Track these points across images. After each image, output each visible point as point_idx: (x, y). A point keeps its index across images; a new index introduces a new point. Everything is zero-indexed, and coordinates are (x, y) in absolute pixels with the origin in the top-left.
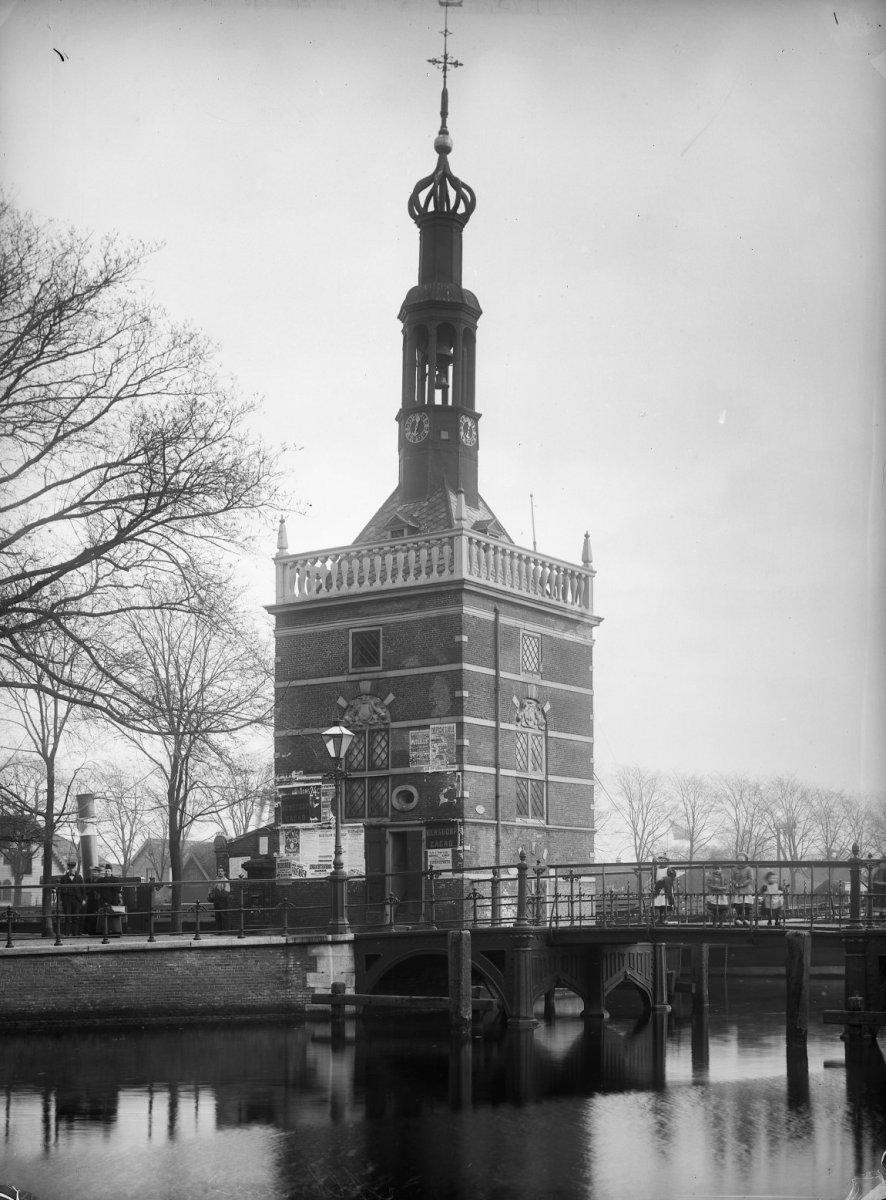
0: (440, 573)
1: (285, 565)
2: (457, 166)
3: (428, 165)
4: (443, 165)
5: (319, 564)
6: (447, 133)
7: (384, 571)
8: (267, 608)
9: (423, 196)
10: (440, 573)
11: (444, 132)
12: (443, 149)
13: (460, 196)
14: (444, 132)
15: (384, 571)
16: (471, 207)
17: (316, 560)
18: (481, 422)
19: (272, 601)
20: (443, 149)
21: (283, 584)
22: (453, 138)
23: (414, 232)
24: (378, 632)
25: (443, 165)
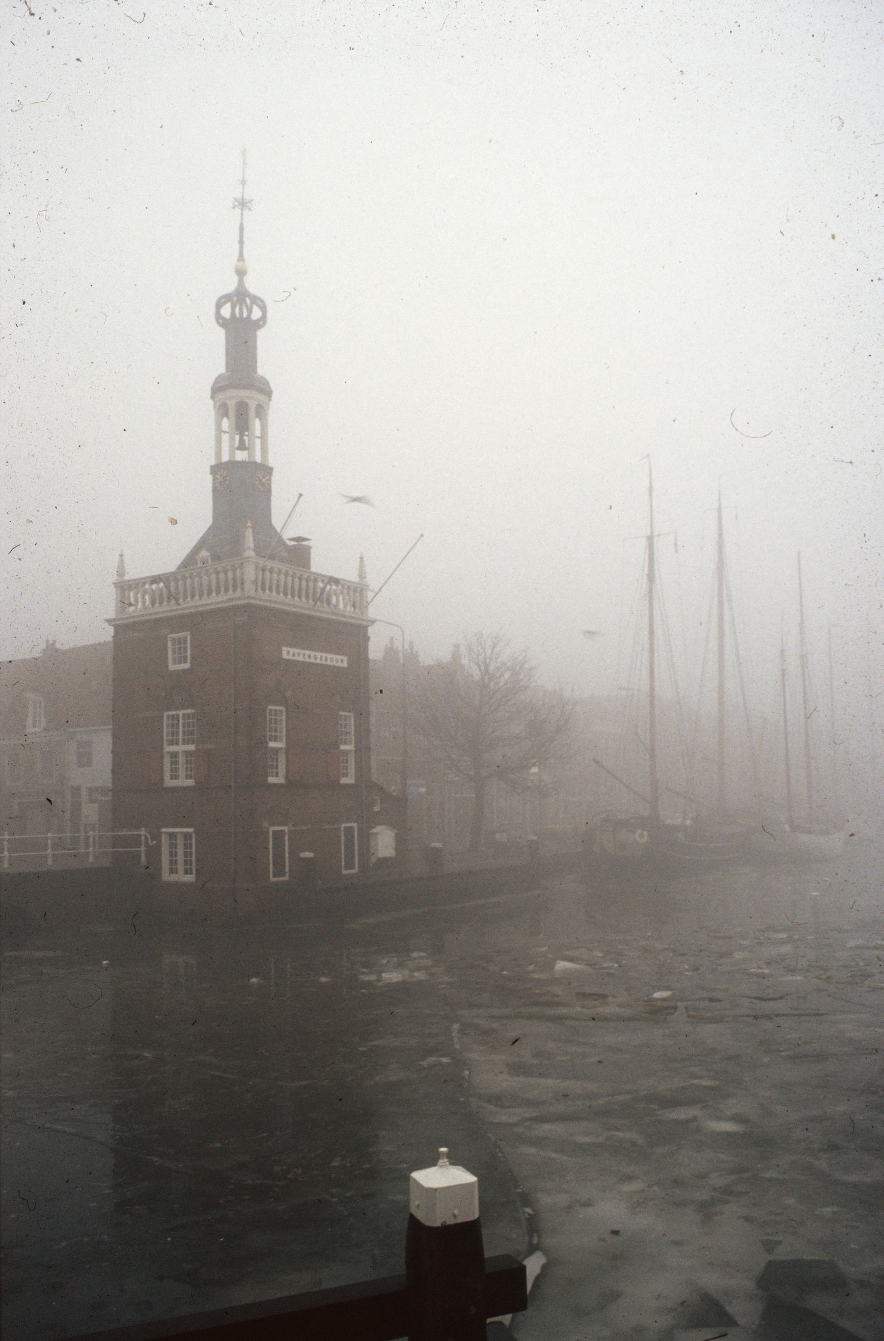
0: (234, 591)
2: (252, 285)
3: (230, 285)
4: (241, 283)
7: (185, 591)
8: (108, 621)
10: (234, 591)
11: (241, 258)
12: (241, 273)
14: (241, 258)
15: (185, 591)
17: (144, 583)
20: (241, 273)
21: (123, 603)
22: (250, 264)
25: (241, 283)
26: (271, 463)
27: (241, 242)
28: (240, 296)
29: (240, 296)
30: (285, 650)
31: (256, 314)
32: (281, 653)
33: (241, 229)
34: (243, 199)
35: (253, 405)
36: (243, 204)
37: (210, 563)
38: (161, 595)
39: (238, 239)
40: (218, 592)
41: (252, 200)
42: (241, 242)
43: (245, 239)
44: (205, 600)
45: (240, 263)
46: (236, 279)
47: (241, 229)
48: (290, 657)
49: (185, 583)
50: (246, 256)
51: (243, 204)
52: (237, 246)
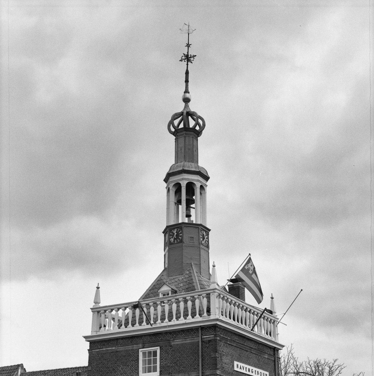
1: (98, 312)
3: (180, 107)
4: (186, 106)
5: (114, 312)
6: (189, 93)
9: (176, 122)
11: (187, 91)
13: (197, 123)
14: (187, 91)
16: (203, 128)
17: (112, 310)
18: (210, 233)
19: (89, 333)
20: (186, 101)
24: (151, 351)
26: (208, 226)
27: (187, 81)
30: (236, 363)
32: (233, 366)
33: (187, 73)
34: (188, 55)
35: (198, 185)
36: (188, 58)
37: (170, 295)
38: (127, 320)
39: (185, 80)
40: (178, 318)
41: (195, 56)
42: (187, 81)
43: (189, 80)
44: (174, 322)
46: (183, 104)
47: (187, 73)
48: (239, 370)
49: (178, 306)
50: (189, 90)
51: (188, 58)
52: (185, 84)
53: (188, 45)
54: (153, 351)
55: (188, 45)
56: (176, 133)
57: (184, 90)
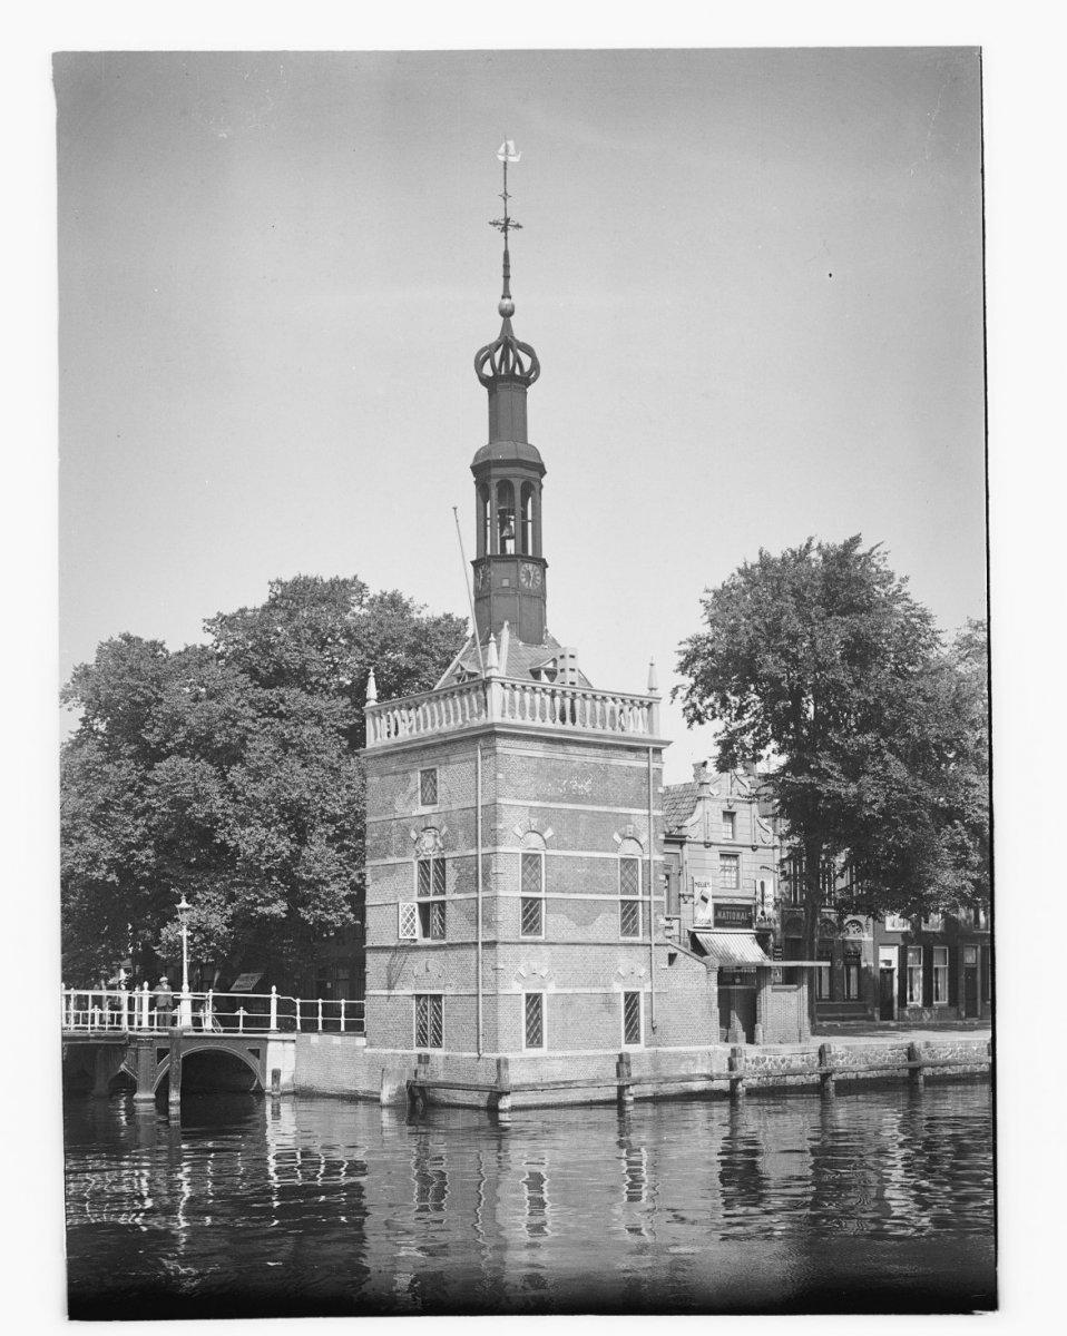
3: (493, 334)
4: (507, 327)
6: (510, 297)
11: (506, 295)
12: (507, 314)
14: (506, 295)
20: (507, 314)
22: (517, 299)
23: (485, 391)
25: (507, 327)
27: (507, 277)
28: (507, 342)
29: (507, 342)
31: (527, 361)
36: (505, 226)
42: (507, 277)
45: (507, 301)
50: (512, 291)
51: (505, 226)
53: (505, 196)
54: (93, 996)
55: (505, 196)
56: (484, 381)
57: (501, 293)
